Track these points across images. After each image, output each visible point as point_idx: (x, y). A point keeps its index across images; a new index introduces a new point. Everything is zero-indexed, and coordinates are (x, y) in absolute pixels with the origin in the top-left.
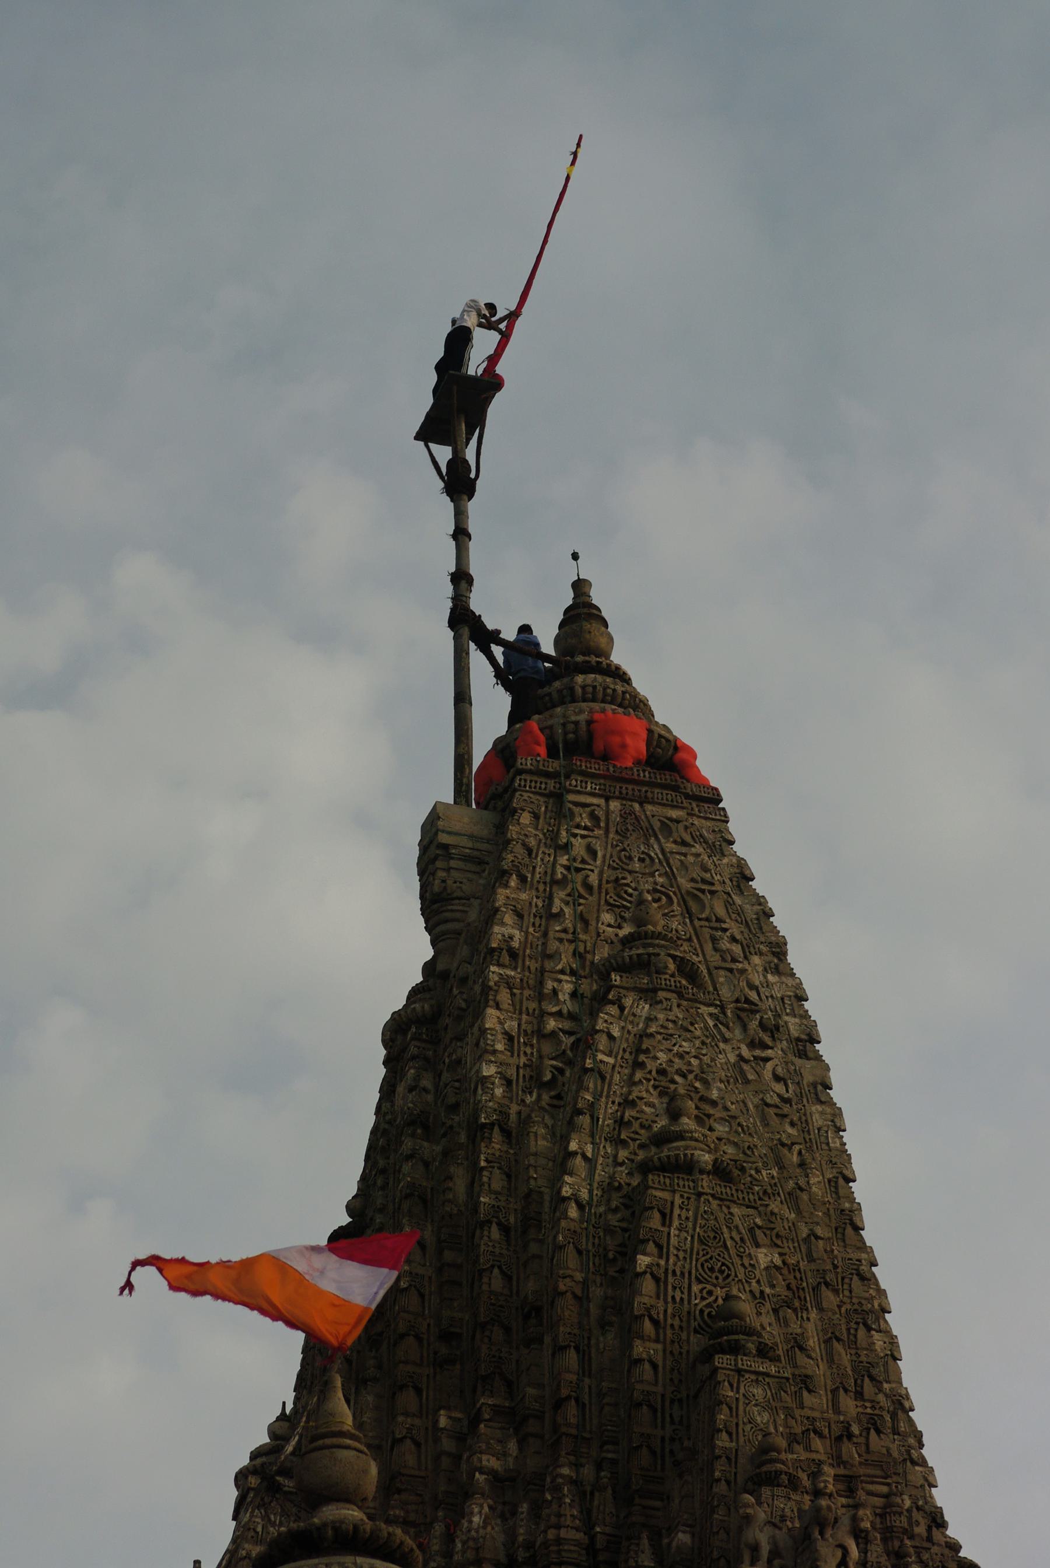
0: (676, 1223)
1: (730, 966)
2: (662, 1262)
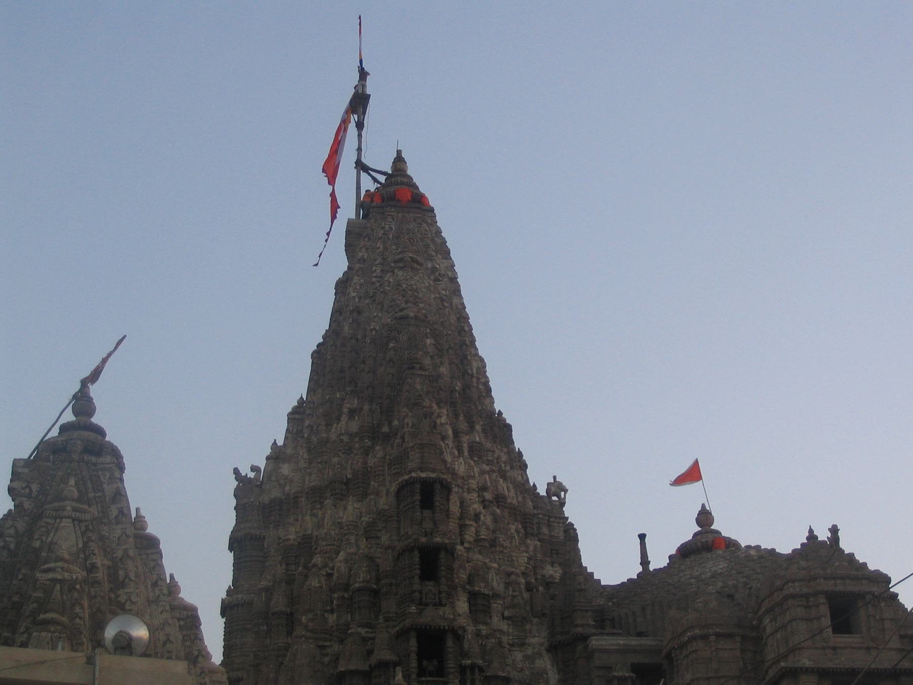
1: (430, 258)
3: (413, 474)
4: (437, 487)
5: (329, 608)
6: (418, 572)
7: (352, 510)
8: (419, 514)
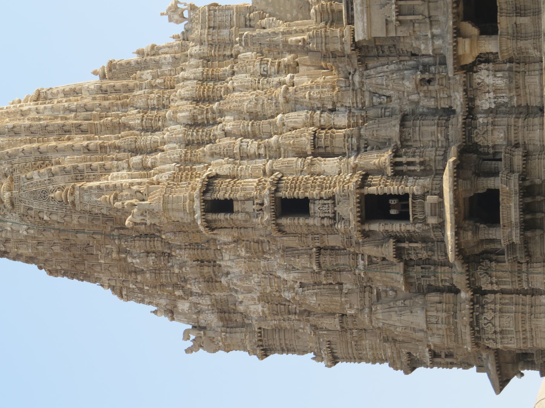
0: (31, 206)
2: (45, 212)
3: (199, 222)
4: (208, 197)
5: (337, 287)
6: (302, 221)
7: (232, 263)
8: (240, 216)
